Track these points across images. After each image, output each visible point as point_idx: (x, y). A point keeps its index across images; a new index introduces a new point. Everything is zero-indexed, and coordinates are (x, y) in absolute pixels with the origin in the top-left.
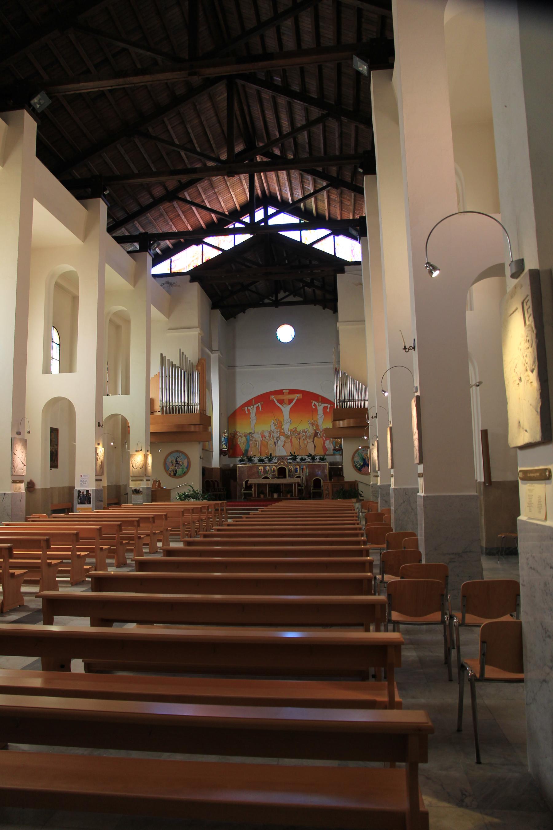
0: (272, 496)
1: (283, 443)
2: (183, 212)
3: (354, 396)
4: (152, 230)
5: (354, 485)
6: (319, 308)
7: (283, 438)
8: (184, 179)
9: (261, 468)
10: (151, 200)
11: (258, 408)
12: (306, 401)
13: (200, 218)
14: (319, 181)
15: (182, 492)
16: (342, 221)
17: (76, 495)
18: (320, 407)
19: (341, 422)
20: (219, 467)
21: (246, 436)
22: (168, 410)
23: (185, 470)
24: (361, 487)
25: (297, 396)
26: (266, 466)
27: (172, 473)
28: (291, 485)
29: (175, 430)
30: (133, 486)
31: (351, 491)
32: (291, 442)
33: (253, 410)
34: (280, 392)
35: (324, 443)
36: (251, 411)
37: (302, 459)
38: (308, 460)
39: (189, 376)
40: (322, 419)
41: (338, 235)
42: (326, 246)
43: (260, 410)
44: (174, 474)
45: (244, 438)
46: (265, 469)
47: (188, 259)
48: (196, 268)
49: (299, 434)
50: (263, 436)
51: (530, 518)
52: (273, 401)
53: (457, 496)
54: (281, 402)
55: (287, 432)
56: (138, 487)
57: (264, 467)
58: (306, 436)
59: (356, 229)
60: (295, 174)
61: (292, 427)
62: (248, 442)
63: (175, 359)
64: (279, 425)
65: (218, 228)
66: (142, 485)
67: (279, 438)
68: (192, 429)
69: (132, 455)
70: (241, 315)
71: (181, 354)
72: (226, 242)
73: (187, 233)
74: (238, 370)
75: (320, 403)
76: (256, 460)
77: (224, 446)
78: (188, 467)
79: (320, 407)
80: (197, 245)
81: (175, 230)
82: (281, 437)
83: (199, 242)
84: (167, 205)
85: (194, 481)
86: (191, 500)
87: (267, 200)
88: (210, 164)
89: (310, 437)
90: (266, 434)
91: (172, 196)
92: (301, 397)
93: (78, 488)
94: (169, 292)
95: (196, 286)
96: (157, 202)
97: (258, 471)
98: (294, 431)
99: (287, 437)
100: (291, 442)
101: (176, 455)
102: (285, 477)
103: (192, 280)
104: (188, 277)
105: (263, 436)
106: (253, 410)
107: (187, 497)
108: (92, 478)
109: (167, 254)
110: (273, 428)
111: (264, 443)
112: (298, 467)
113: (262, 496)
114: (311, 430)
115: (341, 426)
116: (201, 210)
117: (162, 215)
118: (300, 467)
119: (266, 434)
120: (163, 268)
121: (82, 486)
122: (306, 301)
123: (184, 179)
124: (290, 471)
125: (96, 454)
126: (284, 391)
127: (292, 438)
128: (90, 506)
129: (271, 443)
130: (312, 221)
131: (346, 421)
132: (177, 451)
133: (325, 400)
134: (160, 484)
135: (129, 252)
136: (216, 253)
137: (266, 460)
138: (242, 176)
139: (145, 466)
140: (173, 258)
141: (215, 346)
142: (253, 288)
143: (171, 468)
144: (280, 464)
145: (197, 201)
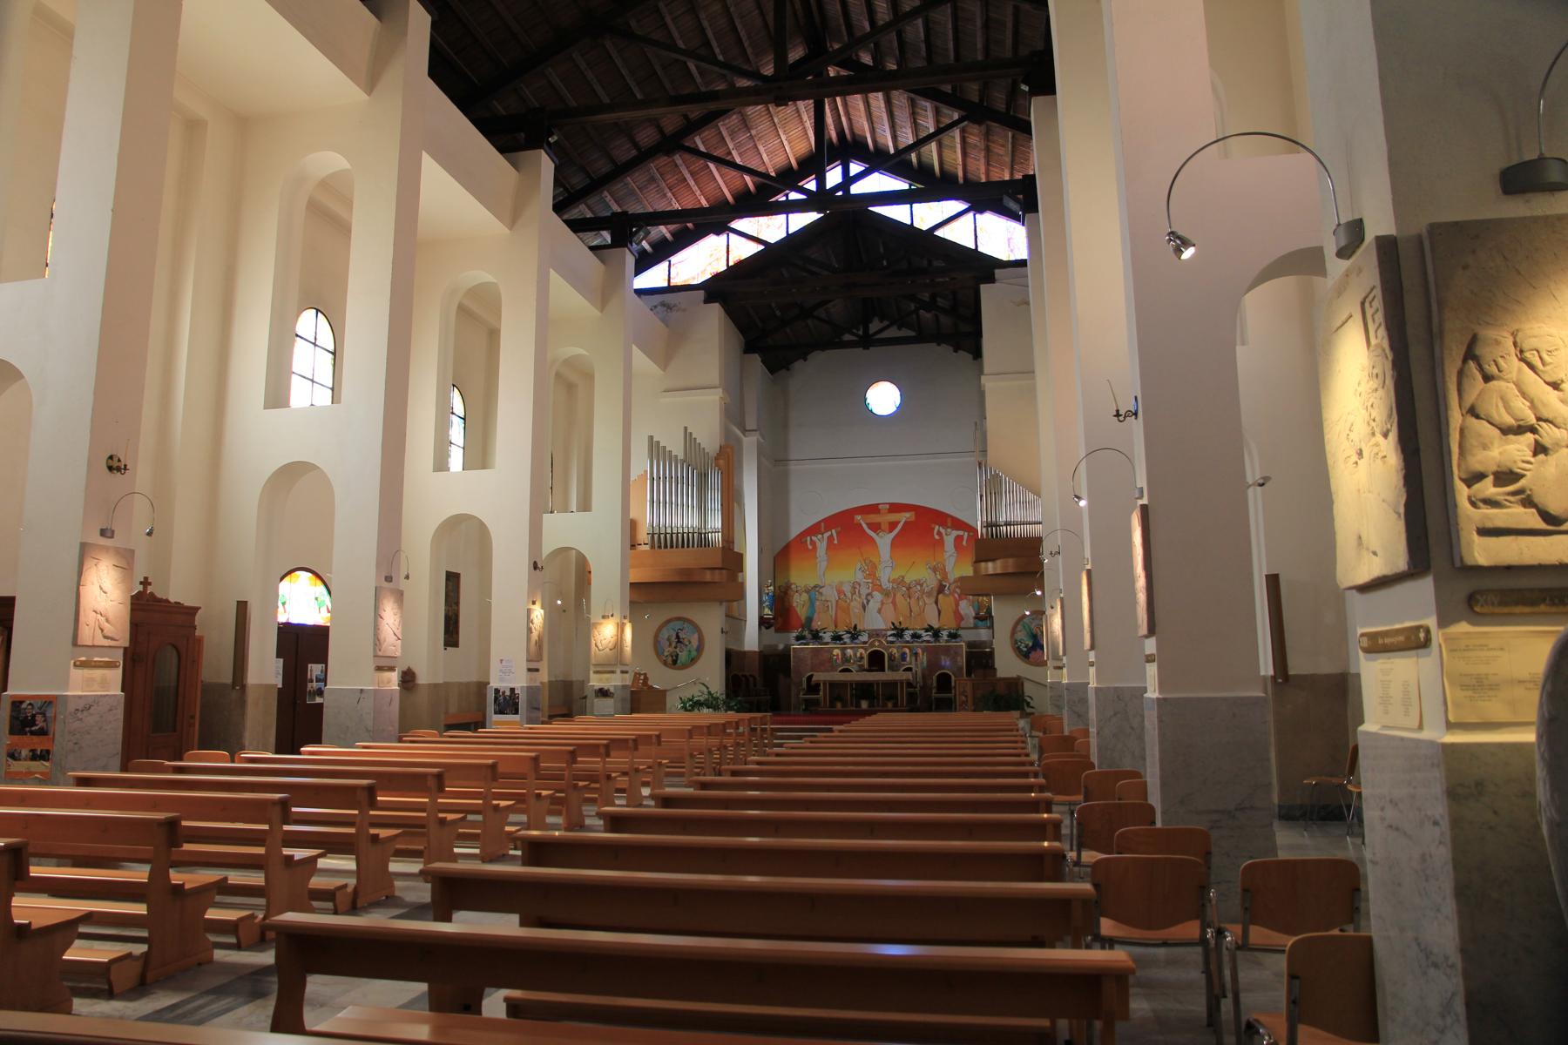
0: (858, 705)
2: (692, 174)
3: (1017, 515)
4: (635, 208)
5: (1015, 684)
6: (945, 350)
7: (878, 596)
8: (695, 111)
9: (836, 652)
10: (634, 152)
11: (830, 538)
12: (922, 525)
13: (724, 184)
14: (946, 110)
15: (687, 695)
16: (989, 184)
17: (491, 696)
18: (950, 537)
19: (990, 564)
20: (756, 648)
21: (807, 591)
22: (664, 541)
23: (694, 653)
24: (1029, 689)
27: (670, 660)
28: (892, 685)
29: (676, 579)
30: (596, 682)
31: (1010, 697)
32: (894, 603)
33: (821, 543)
34: (873, 509)
35: (957, 605)
37: (916, 636)
38: (926, 636)
39: (703, 477)
40: (953, 560)
41: (981, 212)
42: (959, 233)
44: (674, 662)
45: (805, 596)
46: (844, 654)
47: (702, 260)
48: (717, 277)
50: (840, 592)
51: (1385, 727)
53: (1225, 699)
54: (876, 527)
55: (886, 585)
56: (605, 685)
58: (923, 592)
59: (1016, 198)
60: (900, 99)
61: (895, 575)
62: (812, 602)
63: (678, 449)
64: (871, 571)
65: (759, 202)
66: (613, 681)
67: (871, 596)
68: (708, 577)
69: (596, 625)
70: (798, 365)
71: (688, 435)
72: (773, 228)
73: (700, 211)
74: (793, 467)
76: (827, 637)
77: (767, 611)
78: (700, 649)
79: (950, 537)
80: (718, 234)
81: (677, 206)
82: (876, 594)
83: (721, 228)
84: (663, 160)
85: (710, 675)
86: (705, 710)
87: (849, 149)
88: (744, 83)
89: (929, 594)
90: (847, 589)
91: (673, 144)
93: (495, 683)
94: (664, 320)
95: (716, 309)
96: (644, 156)
98: (900, 582)
99: (886, 593)
100: (894, 603)
101: (678, 625)
102: (883, 670)
103: (707, 301)
104: (701, 293)
105: (840, 592)
106: (821, 543)
107: (697, 705)
108: (521, 664)
109: (663, 251)
110: (860, 576)
113: (839, 705)
114: (931, 581)
115: (991, 571)
116: (726, 170)
117: (652, 179)
119: (847, 589)
120: (654, 277)
121: (501, 680)
122: (921, 338)
123: (695, 111)
124: (891, 656)
125: (529, 621)
128: (516, 718)
129: (855, 606)
130: (931, 185)
131: (999, 562)
132: (679, 619)
133: (958, 524)
134: (646, 679)
135: (592, 248)
136: (756, 248)
137: (846, 638)
138: (801, 104)
139: (618, 645)
140: (674, 259)
141: (751, 423)
142: (821, 313)
143: (668, 651)
144: (872, 645)
145: (718, 153)
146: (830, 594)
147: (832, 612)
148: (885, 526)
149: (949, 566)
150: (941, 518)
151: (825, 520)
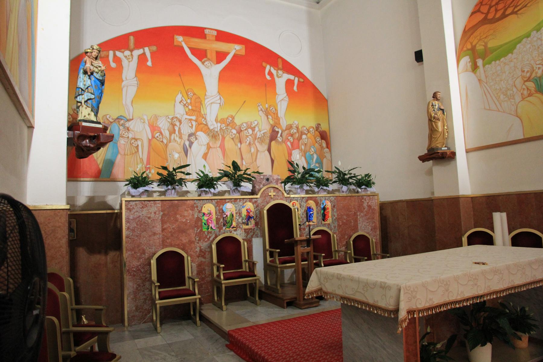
1: (204, 149)
7: (203, 138)
11: (142, 58)
18: (282, 80)
20: (60, 203)
25: (235, 49)
26: (224, 201)
32: (222, 147)
34: (197, 32)
35: (290, 155)
36: (125, 63)
43: (149, 63)
49: (240, 131)
50: (154, 128)
52: (182, 48)
54: (201, 54)
55: (213, 125)
57: (220, 203)
61: (224, 115)
64: (196, 107)
75: (280, 72)
79: (282, 80)
82: (200, 134)
90: (164, 125)
92: (243, 52)
97: (199, 219)
98: (229, 123)
99: (214, 135)
100: (222, 147)
105: (154, 128)
106: (129, 61)
110: (180, 111)
111: (157, 146)
112: (312, 203)
114: (264, 126)
118: (317, 204)
119: (164, 125)
126: (206, 32)
127: (224, 138)
133: (289, 68)
144: (265, 195)
146: (140, 130)
147: (143, 154)
148: (212, 55)
149: (281, 114)
150: (273, 58)
151: (135, 34)
